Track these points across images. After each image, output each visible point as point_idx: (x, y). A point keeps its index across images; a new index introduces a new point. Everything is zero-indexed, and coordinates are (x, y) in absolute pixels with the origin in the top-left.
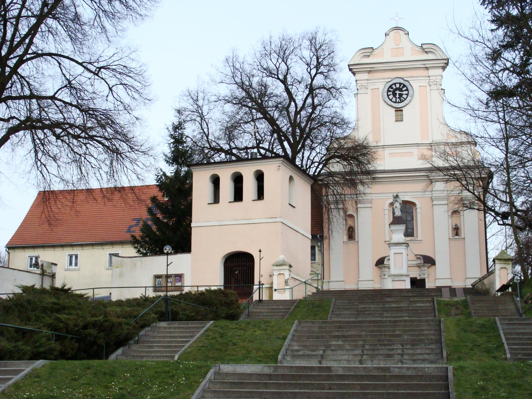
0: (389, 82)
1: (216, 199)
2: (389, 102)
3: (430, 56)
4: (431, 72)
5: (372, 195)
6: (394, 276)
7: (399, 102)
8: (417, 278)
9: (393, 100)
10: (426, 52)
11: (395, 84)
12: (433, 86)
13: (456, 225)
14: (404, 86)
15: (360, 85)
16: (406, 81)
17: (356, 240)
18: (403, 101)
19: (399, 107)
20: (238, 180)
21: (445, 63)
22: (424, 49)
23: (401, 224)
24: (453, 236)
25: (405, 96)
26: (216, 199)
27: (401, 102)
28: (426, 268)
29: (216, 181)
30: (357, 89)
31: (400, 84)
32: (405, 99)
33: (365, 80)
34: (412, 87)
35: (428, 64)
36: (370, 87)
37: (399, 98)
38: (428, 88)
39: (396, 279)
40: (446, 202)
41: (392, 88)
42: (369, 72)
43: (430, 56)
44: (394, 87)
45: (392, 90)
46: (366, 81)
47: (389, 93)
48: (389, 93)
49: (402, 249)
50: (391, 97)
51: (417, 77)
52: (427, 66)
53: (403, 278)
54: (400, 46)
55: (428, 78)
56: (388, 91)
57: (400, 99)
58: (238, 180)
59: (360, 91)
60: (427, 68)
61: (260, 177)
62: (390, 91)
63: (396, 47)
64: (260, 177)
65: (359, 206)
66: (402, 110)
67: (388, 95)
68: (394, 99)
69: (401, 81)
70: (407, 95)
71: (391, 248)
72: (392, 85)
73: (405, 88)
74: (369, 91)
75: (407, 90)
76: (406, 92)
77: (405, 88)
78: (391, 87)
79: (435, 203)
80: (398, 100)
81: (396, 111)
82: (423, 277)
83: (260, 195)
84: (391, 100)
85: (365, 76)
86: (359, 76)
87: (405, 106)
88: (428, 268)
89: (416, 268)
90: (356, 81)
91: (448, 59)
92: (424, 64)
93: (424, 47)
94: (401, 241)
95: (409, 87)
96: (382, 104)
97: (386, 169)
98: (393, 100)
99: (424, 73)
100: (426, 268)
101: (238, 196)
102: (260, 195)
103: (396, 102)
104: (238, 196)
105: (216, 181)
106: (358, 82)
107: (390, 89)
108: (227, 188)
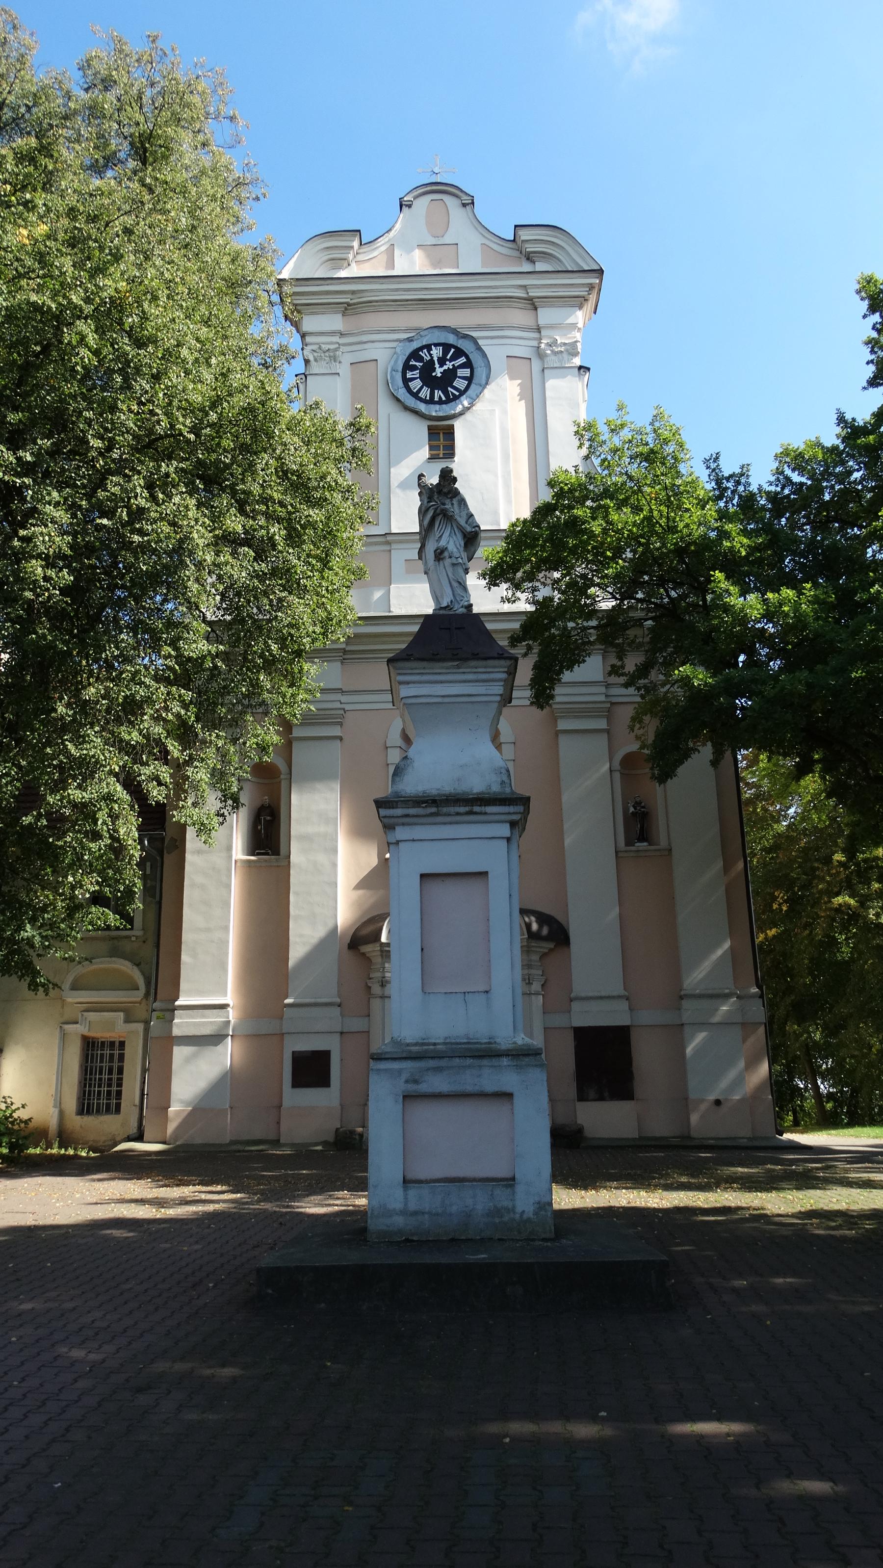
0: (410, 340)
2: (411, 402)
4: (546, 315)
5: (344, 699)
6: (423, 1054)
7: (440, 402)
9: (422, 395)
10: (529, 258)
11: (428, 347)
12: (553, 358)
13: (637, 804)
14: (459, 353)
15: (315, 347)
16: (466, 337)
17: (283, 851)
18: (456, 398)
19: (441, 414)
21: (591, 287)
23: (476, 657)
24: (629, 843)
25: (460, 384)
27: (449, 401)
30: (307, 362)
31: (446, 347)
32: (462, 393)
33: (332, 333)
34: (484, 355)
35: (538, 287)
36: (347, 359)
38: (536, 365)
39: (438, 1083)
40: (602, 724)
41: (421, 359)
42: (347, 309)
44: (424, 354)
45: (419, 364)
46: (336, 339)
47: (409, 375)
48: (409, 375)
49: (476, 845)
50: (416, 385)
51: (501, 328)
52: (532, 294)
53: (492, 1078)
54: (447, 239)
55: (536, 335)
56: (407, 367)
57: (446, 393)
59: (315, 368)
60: (532, 304)
62: (414, 368)
63: (432, 241)
65: (296, 733)
67: (406, 381)
68: (425, 393)
69: (451, 339)
70: (470, 380)
71: (401, 833)
72: (421, 349)
73: (463, 360)
74: (344, 369)
75: (469, 364)
76: (466, 372)
77: (463, 360)
78: (415, 355)
79: (562, 725)
81: (430, 428)
84: (415, 395)
85: (334, 322)
86: (309, 323)
87: (461, 414)
88: (543, 956)
91: (601, 272)
92: (525, 287)
93: (524, 235)
94: (476, 785)
95: (475, 358)
96: (385, 407)
97: (396, 611)
98: (422, 395)
99: (520, 316)
103: (431, 401)
106: (308, 339)
107: (413, 363)
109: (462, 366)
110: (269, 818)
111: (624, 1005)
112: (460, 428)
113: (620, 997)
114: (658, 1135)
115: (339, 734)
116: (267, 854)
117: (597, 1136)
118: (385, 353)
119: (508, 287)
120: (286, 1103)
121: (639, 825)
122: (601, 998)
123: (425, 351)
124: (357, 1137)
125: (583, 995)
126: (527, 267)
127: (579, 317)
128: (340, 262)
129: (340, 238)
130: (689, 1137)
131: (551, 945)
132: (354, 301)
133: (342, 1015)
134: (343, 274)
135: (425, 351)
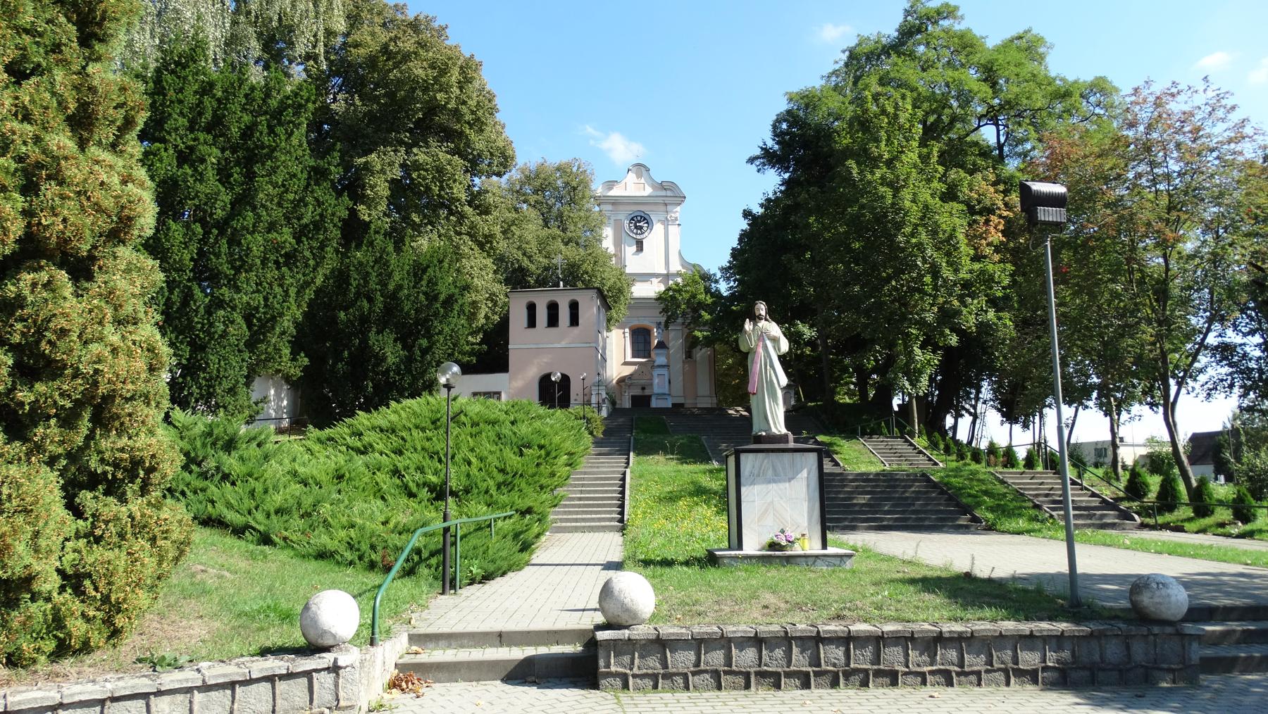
1: (532, 323)
3: (669, 193)
4: (669, 208)
20: (553, 308)
22: (662, 186)
26: (532, 323)
29: (531, 308)
35: (667, 200)
42: (613, 204)
43: (669, 193)
49: (664, 371)
58: (553, 308)
61: (574, 306)
64: (574, 306)
74: (612, 221)
83: (574, 321)
85: (610, 207)
86: (604, 207)
99: (663, 208)
101: (553, 321)
102: (574, 321)
104: (553, 321)
105: (531, 308)
108: (542, 315)
118: (623, 216)
119: (660, 200)
121: (689, 355)
126: (663, 193)
127: (678, 209)
128: (610, 189)
129: (611, 184)
132: (616, 202)
134: (611, 193)
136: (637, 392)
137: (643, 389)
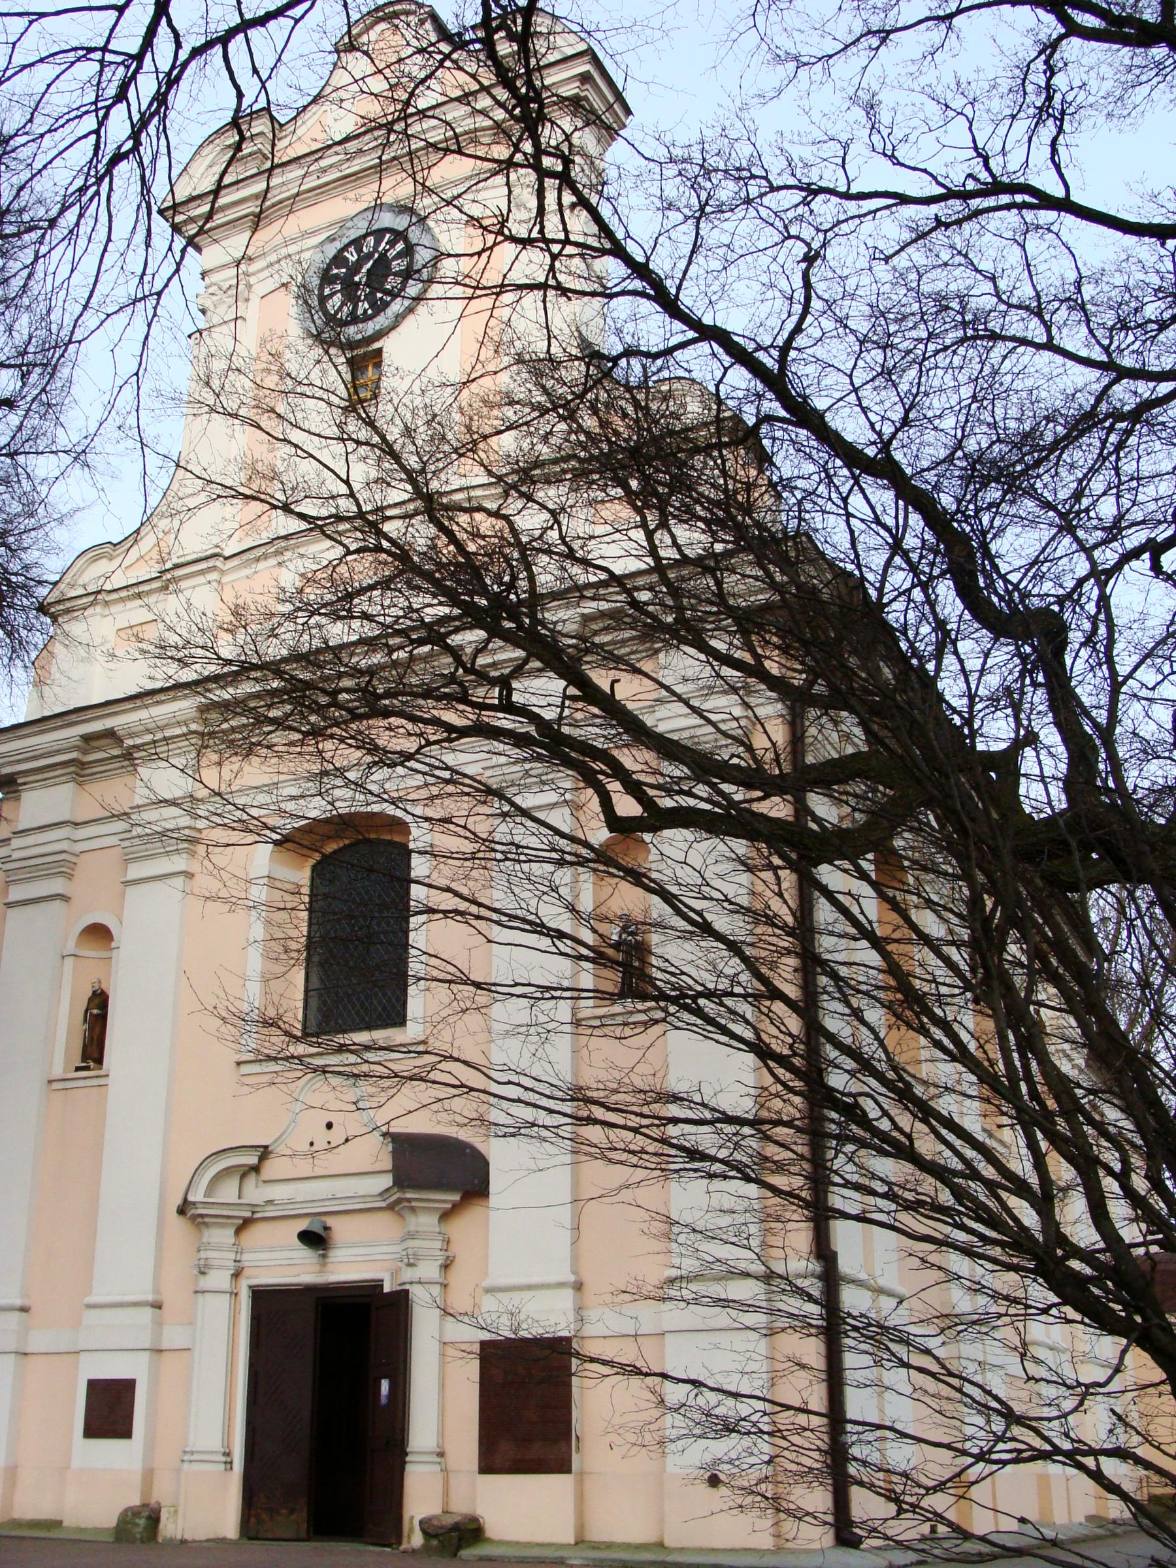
0: (331, 239)
7: (367, 318)
8: (377, 1285)
11: (357, 243)
21: (585, 78)
25: (391, 283)
28: (427, 1222)
37: (370, 298)
44: (352, 256)
66: (379, 352)
73: (400, 246)
80: (363, 306)
82: (408, 1274)
88: (445, 1216)
89: (386, 1218)
90: (204, 275)
100: (427, 1222)
109: (399, 255)
110: (95, 1011)
111: (567, 1298)
112: (390, 346)
113: (561, 1285)
114: (619, 1538)
115: (183, 868)
116: (87, 1068)
117: (508, 1538)
120: (76, 1463)
122: (530, 1287)
123: (352, 249)
124: (142, 1522)
125: (502, 1282)
130: (660, 1545)
131: (456, 1197)
133: (158, 1324)
135: (352, 249)
136: (285, 1264)
137: (316, 1239)
